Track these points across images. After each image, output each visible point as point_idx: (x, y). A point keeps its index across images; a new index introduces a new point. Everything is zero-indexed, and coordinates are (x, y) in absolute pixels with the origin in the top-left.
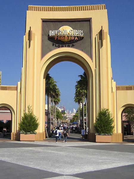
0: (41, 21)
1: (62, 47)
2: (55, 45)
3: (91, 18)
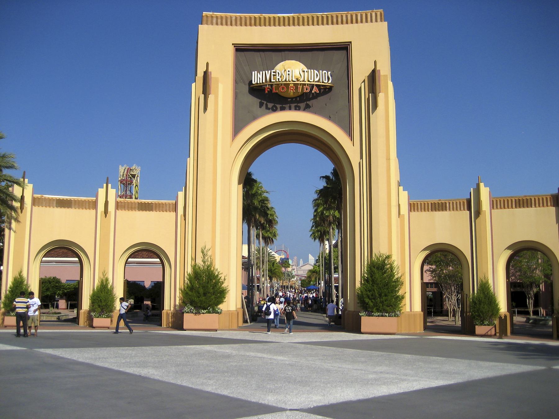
0: (232, 49)
1: (282, 109)
2: (266, 105)
3: (351, 42)
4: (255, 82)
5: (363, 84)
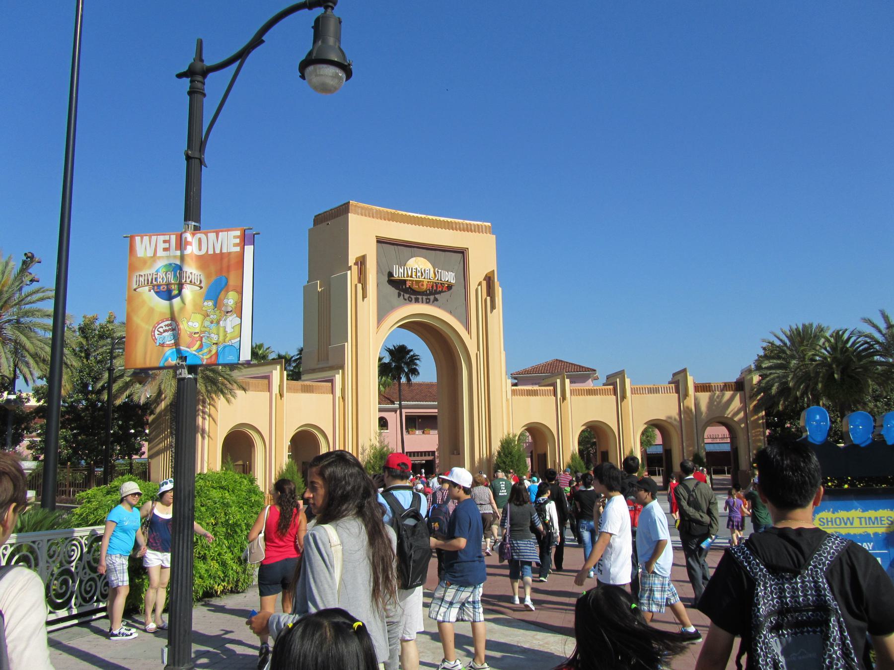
3: (468, 249)
5: (480, 287)
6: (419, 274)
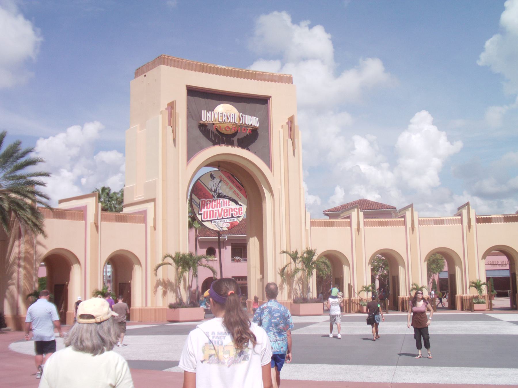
4: (204, 119)
6: (225, 118)
